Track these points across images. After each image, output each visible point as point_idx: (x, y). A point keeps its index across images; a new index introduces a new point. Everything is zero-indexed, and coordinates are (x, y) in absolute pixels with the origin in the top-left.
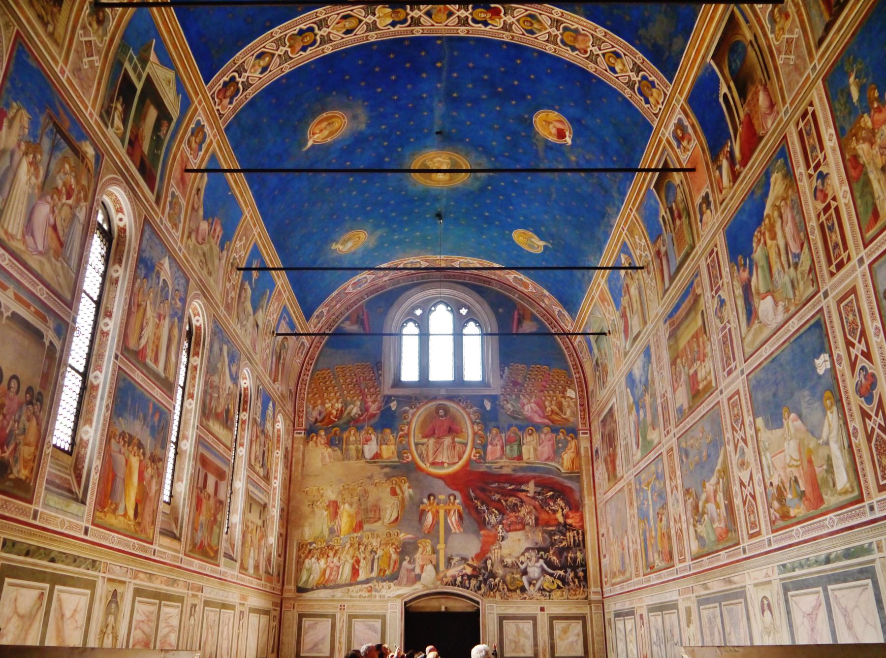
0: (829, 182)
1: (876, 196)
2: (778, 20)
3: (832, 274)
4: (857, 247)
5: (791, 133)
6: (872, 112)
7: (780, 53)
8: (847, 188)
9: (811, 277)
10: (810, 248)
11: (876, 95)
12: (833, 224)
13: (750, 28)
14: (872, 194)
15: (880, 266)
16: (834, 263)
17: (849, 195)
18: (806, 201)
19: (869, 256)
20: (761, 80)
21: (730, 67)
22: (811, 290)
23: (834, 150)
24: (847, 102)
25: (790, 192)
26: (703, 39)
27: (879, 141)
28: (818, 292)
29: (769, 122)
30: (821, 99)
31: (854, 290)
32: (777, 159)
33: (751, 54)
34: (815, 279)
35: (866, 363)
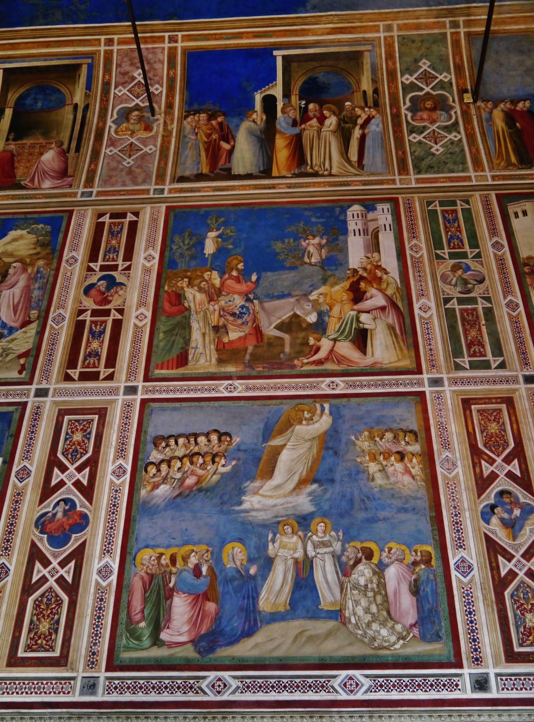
0: (121, 292)
1: (193, 344)
2: (132, 121)
3: (68, 378)
4: (131, 373)
5: (84, 216)
6: (227, 276)
7: (112, 143)
8: (149, 314)
9: (22, 361)
10: (41, 333)
11: (241, 266)
12: (103, 332)
13: (87, 96)
14: (187, 341)
15: (163, 409)
16: (79, 369)
17: (148, 321)
18: (66, 288)
19: (146, 391)
20: (62, 144)
21: (22, 98)
22: (14, 375)
23: (147, 271)
24: (194, 246)
25: (41, 263)
26: (13, 46)
27: (223, 303)
28: (30, 383)
29: (47, 184)
30: (154, 220)
31: (102, 413)
32: (46, 221)
33: (67, 113)
34: (29, 366)
35: (78, 498)
